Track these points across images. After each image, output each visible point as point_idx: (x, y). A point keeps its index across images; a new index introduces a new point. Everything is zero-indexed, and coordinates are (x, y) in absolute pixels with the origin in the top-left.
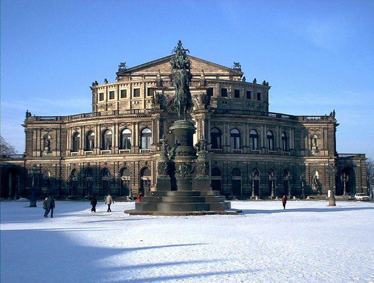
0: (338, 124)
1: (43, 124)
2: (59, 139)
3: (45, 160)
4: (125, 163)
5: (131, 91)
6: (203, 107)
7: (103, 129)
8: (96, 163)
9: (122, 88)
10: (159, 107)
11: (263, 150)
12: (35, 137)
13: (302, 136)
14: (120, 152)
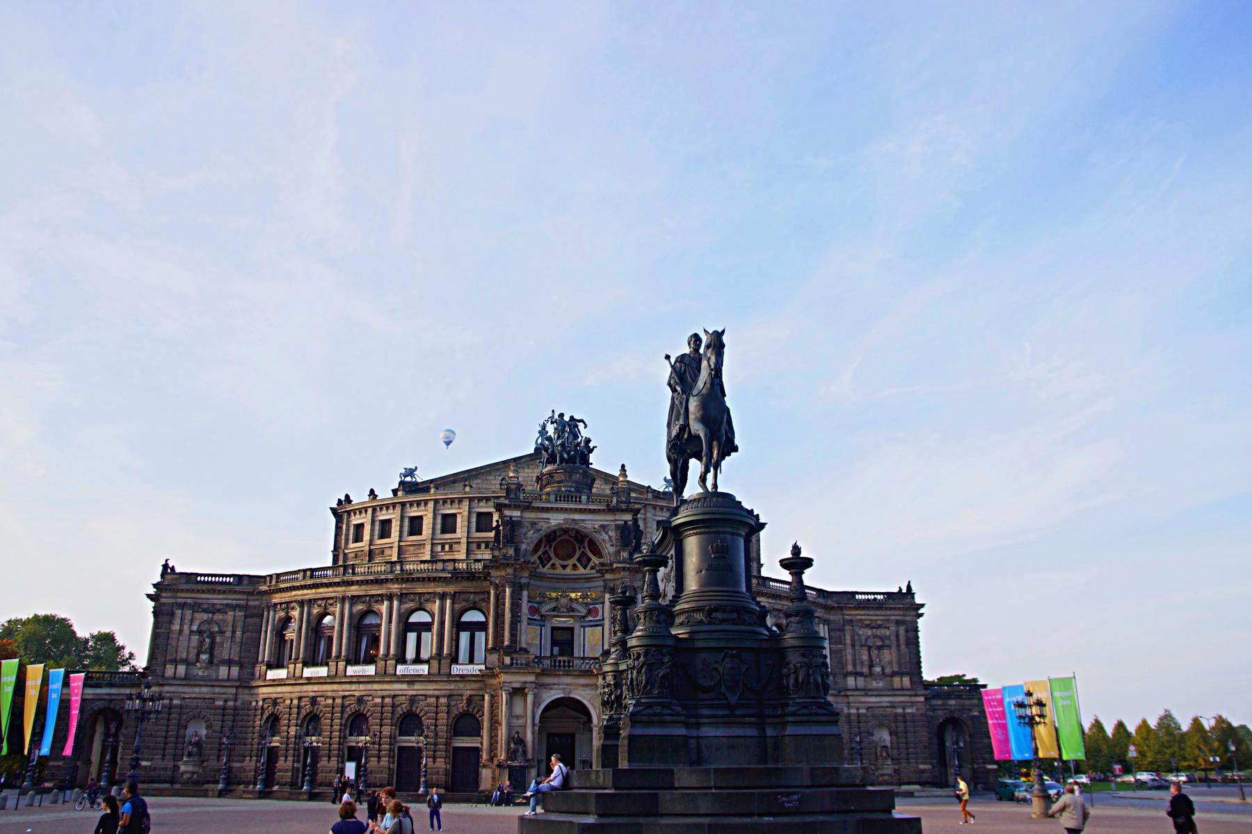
0: (921, 615)
1: (203, 592)
2: (239, 634)
3: (197, 690)
4: (413, 700)
5: (435, 518)
6: (625, 555)
7: (360, 607)
8: (334, 699)
9: (414, 512)
10: (511, 552)
12: (176, 627)
13: (848, 641)
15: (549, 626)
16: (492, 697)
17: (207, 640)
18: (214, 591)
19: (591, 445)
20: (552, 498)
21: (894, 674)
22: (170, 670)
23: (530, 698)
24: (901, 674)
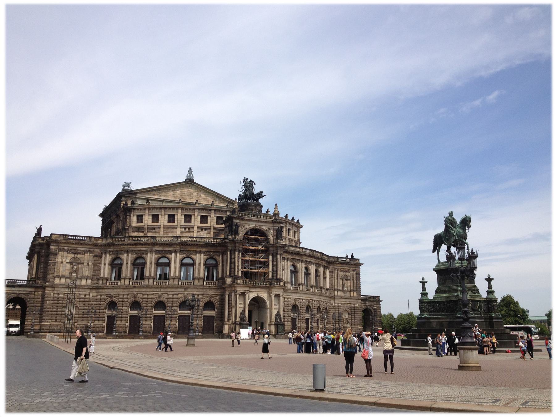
2: (90, 264)
12: (59, 260)
13: (336, 277)
14: (180, 283)
16: (229, 295)
17: (75, 267)
18: (78, 244)
19: (263, 194)
20: (250, 216)
21: (350, 291)
22: (57, 281)
23: (247, 297)
24: (354, 291)
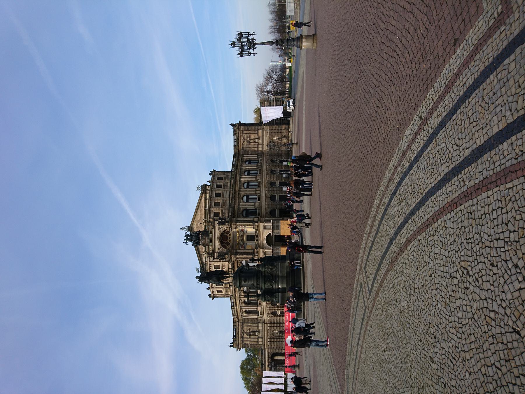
2: (250, 324)
6: (227, 224)
10: (227, 256)
11: (258, 178)
12: (248, 343)
15: (246, 242)
22: (260, 343)
24: (258, 134)
